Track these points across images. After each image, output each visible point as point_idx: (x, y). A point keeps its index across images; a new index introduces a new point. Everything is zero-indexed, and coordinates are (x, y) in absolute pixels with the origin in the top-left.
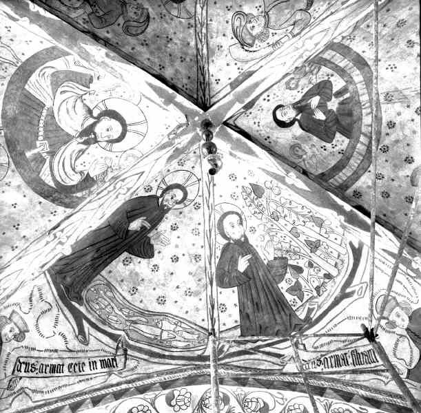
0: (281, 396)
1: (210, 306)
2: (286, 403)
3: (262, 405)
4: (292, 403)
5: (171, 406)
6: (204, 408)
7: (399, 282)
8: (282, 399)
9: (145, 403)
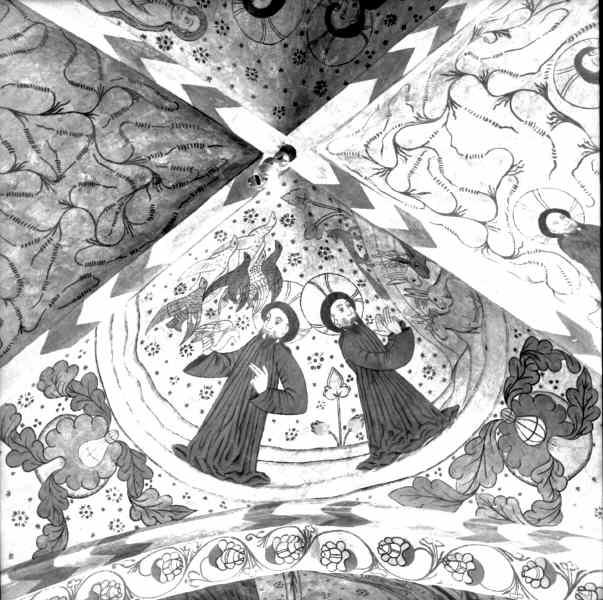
0: (194, 583)
1: (297, 585)
2: (186, 576)
3: (219, 562)
4: (178, 578)
5: (348, 551)
6: (302, 537)
7: (40, 480)
8: (191, 580)
9: (386, 565)
